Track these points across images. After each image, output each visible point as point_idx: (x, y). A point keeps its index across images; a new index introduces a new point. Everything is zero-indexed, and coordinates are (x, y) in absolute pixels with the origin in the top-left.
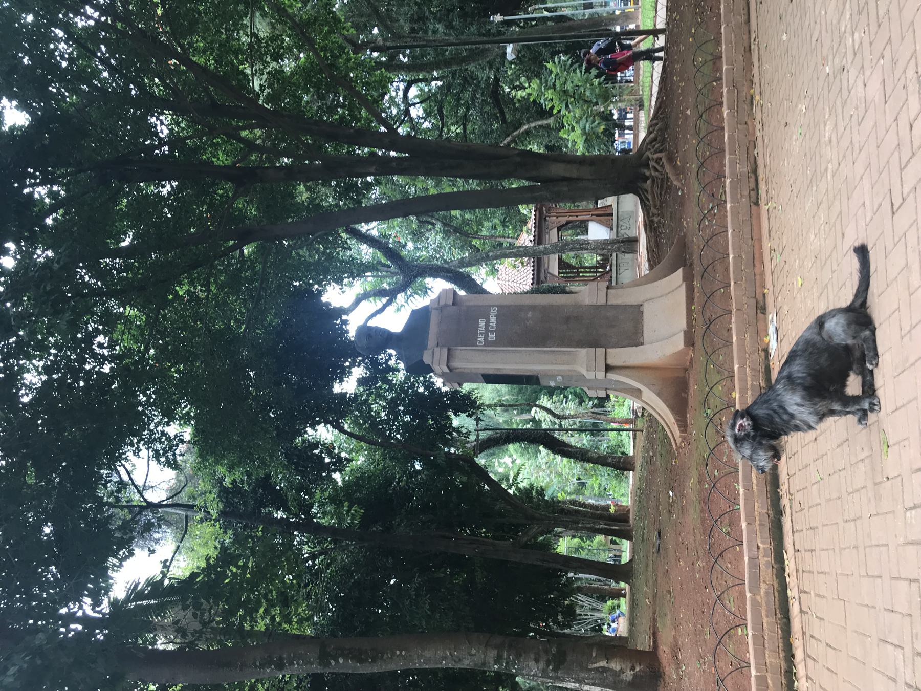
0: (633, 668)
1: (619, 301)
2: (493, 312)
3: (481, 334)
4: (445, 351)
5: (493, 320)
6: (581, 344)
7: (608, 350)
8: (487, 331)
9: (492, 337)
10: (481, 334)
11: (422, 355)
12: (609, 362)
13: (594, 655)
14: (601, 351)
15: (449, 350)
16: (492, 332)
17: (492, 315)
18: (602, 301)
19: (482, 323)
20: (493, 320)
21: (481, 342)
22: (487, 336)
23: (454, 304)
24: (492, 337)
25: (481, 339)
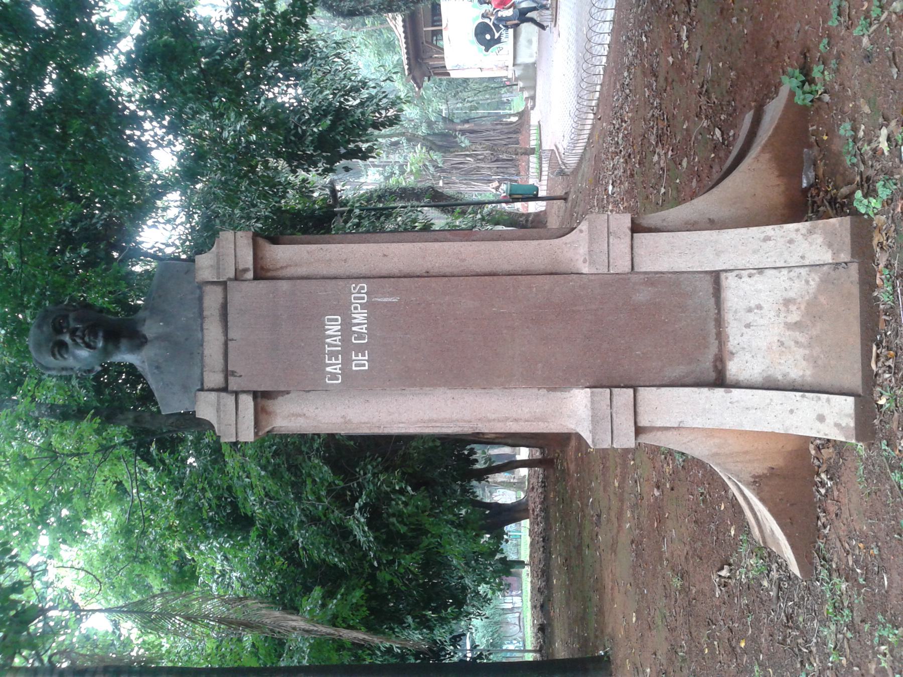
1: (664, 264)
2: (359, 293)
3: (333, 354)
5: (360, 317)
7: (642, 391)
8: (347, 348)
11: (194, 402)
12: (643, 422)
14: (624, 396)
16: (360, 349)
17: (356, 303)
18: (622, 265)
19: (333, 328)
20: (360, 317)
21: (334, 376)
22: (347, 362)
24: (361, 362)
25: (334, 367)
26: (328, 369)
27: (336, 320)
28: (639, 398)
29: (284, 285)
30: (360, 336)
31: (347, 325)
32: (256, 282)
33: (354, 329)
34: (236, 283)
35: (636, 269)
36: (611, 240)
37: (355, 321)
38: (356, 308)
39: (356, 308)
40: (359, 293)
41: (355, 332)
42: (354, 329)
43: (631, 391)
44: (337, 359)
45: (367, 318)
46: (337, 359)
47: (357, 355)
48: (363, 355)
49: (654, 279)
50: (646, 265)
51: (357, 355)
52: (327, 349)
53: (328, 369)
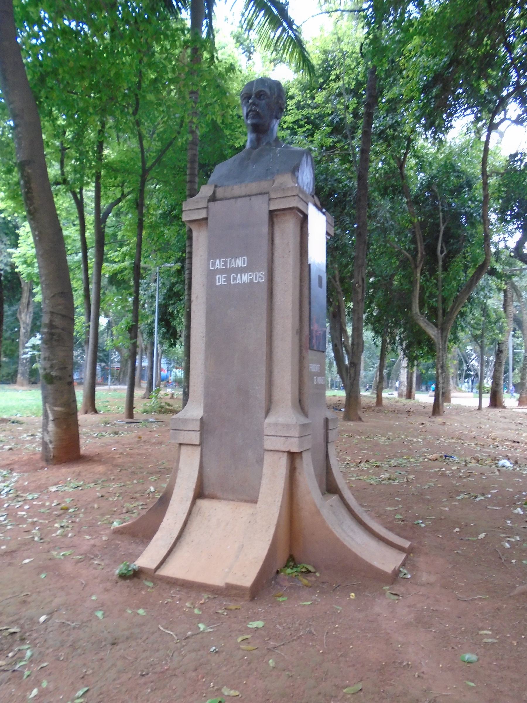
0: (51, 442)
1: (266, 470)
3: (225, 262)
4: (202, 214)
5: (246, 278)
6: (209, 408)
8: (227, 271)
9: (220, 280)
10: (225, 262)
13: (56, 409)
14: (195, 438)
15: (206, 219)
16: (228, 279)
18: (269, 443)
19: (240, 262)
20: (246, 278)
21: (214, 264)
23: (272, 214)
24: (220, 280)
25: (219, 264)
26: (218, 261)
27: (244, 264)
28: (195, 448)
29: (265, 229)
30: (235, 279)
31: (241, 270)
32: (267, 212)
33: (239, 275)
34: (267, 199)
35: (266, 453)
36: (282, 438)
37: (243, 275)
38: (250, 275)
39: (250, 275)
40: (259, 277)
41: (237, 275)
42: (239, 275)
43: (198, 443)
44: (223, 266)
45: (244, 283)
46: (223, 266)
47: (224, 277)
48: (224, 281)
49: (260, 461)
50: (268, 459)
51: (224, 277)
52: (228, 259)
53: (218, 261)
